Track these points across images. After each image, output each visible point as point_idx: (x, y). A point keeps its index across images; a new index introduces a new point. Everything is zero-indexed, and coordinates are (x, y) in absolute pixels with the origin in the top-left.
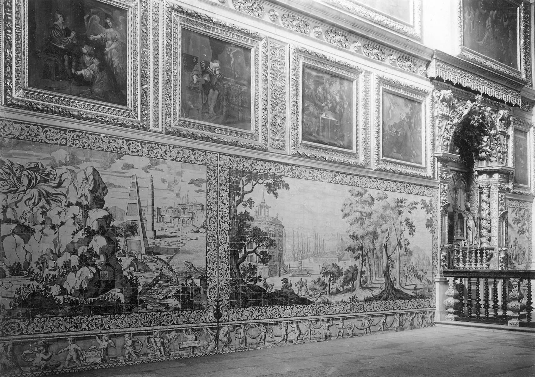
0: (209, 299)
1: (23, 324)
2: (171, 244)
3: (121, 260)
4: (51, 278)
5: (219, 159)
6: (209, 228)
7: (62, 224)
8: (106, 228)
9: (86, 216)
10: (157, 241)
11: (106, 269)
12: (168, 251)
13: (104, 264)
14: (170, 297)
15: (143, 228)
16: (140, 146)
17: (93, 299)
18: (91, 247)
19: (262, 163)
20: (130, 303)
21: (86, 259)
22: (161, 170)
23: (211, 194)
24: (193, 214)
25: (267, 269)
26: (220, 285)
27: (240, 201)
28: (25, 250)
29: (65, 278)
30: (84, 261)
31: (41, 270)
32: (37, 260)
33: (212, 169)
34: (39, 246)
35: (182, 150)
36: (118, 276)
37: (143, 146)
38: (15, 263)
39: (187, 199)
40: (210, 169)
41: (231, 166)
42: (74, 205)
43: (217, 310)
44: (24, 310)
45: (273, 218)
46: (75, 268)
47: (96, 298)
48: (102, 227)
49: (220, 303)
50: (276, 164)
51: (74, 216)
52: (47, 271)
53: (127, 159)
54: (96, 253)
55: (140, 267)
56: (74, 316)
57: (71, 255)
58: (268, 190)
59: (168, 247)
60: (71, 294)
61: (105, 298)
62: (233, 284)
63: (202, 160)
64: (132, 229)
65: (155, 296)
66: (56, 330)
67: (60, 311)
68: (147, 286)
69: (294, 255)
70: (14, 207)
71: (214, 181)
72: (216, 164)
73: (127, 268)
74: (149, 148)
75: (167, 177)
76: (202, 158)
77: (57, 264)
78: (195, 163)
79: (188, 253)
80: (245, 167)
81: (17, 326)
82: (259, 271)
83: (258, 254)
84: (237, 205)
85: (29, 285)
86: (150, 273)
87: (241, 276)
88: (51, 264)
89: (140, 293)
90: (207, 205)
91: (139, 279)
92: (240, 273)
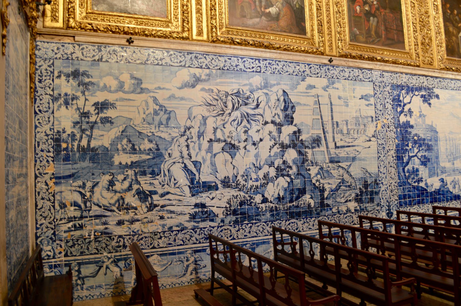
0: (382, 200)
1: (234, 230)
2: (349, 153)
3: (309, 170)
4: (255, 189)
5: (382, 76)
6: (379, 137)
7: (261, 140)
8: (296, 142)
9: (280, 132)
10: (338, 151)
12: (347, 159)
13: (296, 174)
14: (350, 200)
15: (326, 140)
16: (319, 69)
17: (289, 205)
19: (417, 77)
20: (319, 207)
21: (282, 170)
22: (338, 89)
23: (378, 106)
25: (427, 170)
26: (390, 187)
27: (402, 112)
30: (280, 172)
31: (246, 182)
32: (243, 173)
33: (378, 85)
34: (244, 160)
35: (353, 71)
36: (308, 183)
37: (322, 68)
38: (225, 177)
40: (376, 85)
41: (392, 82)
43: (388, 210)
44: (234, 218)
45: (429, 125)
46: (273, 178)
48: (293, 141)
49: (391, 203)
50: (428, 78)
51: (270, 132)
52: (251, 183)
53: (310, 81)
55: (326, 175)
56: (274, 221)
57: (270, 167)
58: (424, 101)
59: (347, 156)
60: (271, 202)
62: (401, 186)
63: (369, 78)
64: (317, 141)
65: (338, 200)
66: (260, 234)
67: (263, 217)
68: (332, 191)
69: (447, 157)
71: (380, 96)
72: (380, 80)
73: (314, 177)
74: (327, 71)
75: (342, 94)
76: (369, 76)
77: (258, 176)
78: (364, 81)
79: (364, 160)
80: (403, 82)
81: (229, 232)
82: (420, 173)
83: (420, 158)
84: (400, 115)
85: (237, 196)
87: (407, 178)
88: (254, 176)
89: (327, 198)
90: (376, 117)
92: (405, 175)
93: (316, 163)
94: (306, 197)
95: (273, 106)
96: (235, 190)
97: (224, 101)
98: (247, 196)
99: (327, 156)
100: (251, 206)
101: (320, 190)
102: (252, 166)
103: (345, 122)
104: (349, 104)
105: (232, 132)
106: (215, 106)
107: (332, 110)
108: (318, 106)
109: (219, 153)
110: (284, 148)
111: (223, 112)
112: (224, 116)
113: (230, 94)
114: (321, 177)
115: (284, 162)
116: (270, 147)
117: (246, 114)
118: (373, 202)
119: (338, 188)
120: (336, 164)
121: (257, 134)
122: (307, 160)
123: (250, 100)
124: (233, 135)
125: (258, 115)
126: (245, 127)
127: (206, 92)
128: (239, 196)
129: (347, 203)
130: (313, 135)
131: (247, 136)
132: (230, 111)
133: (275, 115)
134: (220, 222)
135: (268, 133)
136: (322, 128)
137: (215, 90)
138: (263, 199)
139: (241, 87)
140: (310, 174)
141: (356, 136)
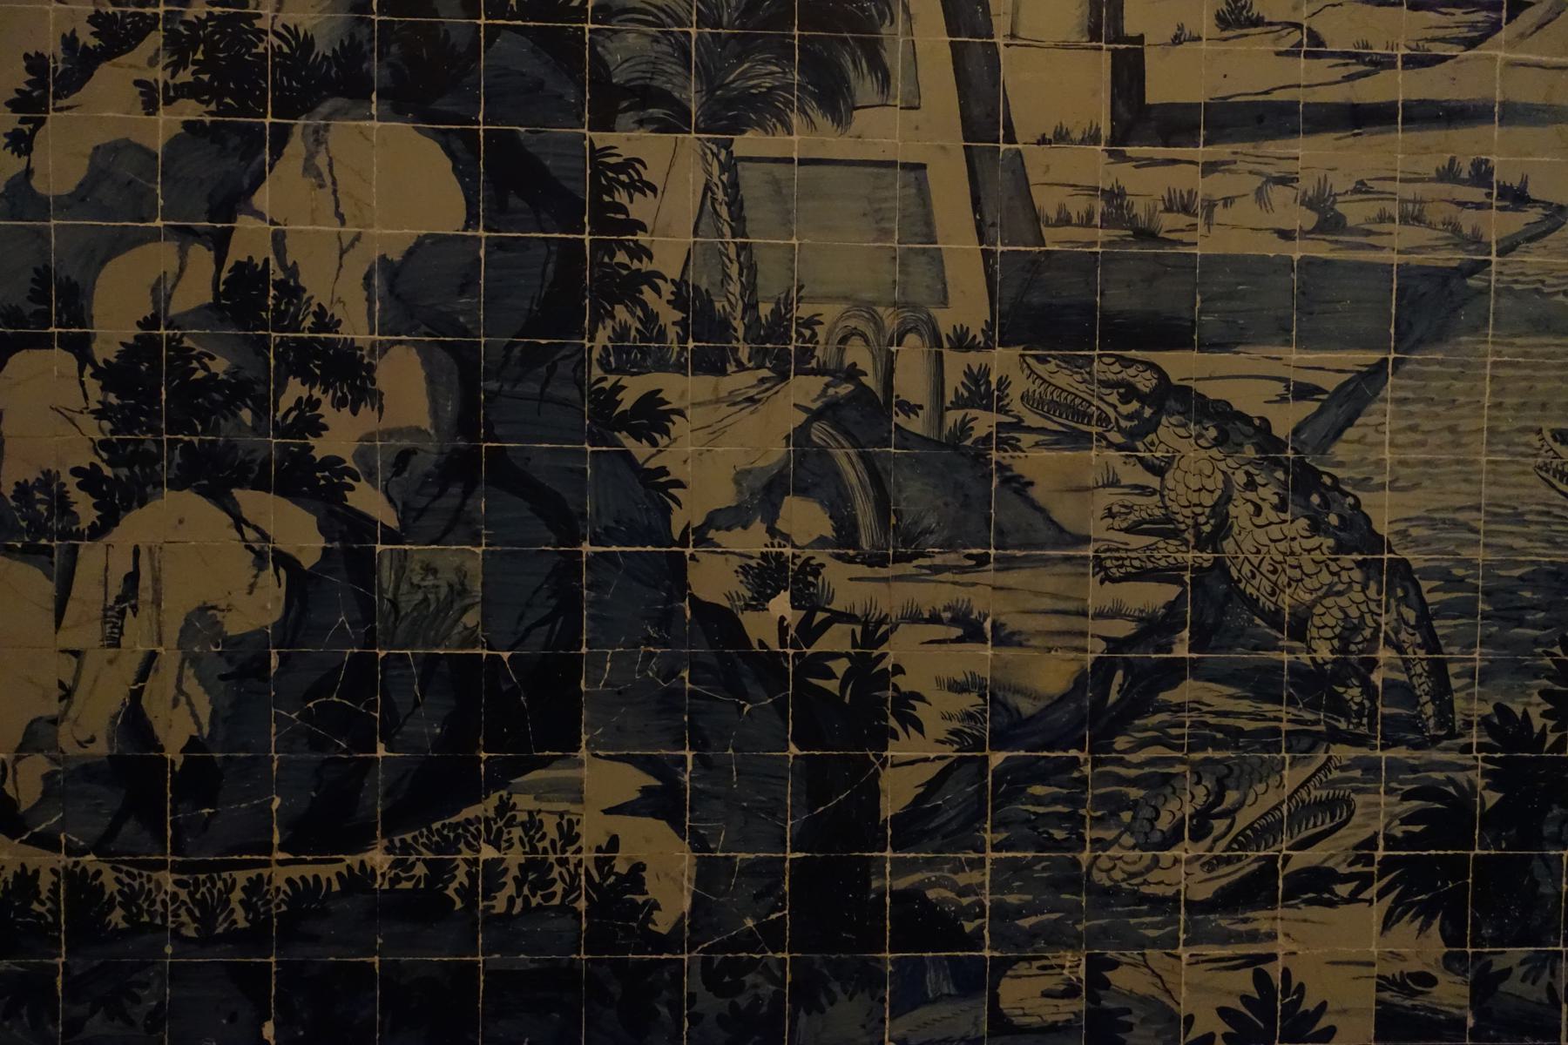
2: (1355, 212)
3: (653, 417)
10: (1150, 180)
11: (458, 527)
12: (1306, 301)
13: (425, 462)
17: (282, 874)
18: (262, 251)
20: (771, 935)
21: (200, 401)
46: (62, 505)
47: (327, 872)
54: (324, 321)
59: (1321, 250)
61: (440, 871)
65: (1114, 858)
73: (734, 518)
86: (1048, 580)
89: (913, 826)
93: (778, 327)
94: (575, 793)
110: (250, 101)
114: (845, 536)
116: (20, 77)
119: (1124, 687)
120: (1104, 367)
122: (628, 287)
129: (1262, 920)
140: (658, 487)
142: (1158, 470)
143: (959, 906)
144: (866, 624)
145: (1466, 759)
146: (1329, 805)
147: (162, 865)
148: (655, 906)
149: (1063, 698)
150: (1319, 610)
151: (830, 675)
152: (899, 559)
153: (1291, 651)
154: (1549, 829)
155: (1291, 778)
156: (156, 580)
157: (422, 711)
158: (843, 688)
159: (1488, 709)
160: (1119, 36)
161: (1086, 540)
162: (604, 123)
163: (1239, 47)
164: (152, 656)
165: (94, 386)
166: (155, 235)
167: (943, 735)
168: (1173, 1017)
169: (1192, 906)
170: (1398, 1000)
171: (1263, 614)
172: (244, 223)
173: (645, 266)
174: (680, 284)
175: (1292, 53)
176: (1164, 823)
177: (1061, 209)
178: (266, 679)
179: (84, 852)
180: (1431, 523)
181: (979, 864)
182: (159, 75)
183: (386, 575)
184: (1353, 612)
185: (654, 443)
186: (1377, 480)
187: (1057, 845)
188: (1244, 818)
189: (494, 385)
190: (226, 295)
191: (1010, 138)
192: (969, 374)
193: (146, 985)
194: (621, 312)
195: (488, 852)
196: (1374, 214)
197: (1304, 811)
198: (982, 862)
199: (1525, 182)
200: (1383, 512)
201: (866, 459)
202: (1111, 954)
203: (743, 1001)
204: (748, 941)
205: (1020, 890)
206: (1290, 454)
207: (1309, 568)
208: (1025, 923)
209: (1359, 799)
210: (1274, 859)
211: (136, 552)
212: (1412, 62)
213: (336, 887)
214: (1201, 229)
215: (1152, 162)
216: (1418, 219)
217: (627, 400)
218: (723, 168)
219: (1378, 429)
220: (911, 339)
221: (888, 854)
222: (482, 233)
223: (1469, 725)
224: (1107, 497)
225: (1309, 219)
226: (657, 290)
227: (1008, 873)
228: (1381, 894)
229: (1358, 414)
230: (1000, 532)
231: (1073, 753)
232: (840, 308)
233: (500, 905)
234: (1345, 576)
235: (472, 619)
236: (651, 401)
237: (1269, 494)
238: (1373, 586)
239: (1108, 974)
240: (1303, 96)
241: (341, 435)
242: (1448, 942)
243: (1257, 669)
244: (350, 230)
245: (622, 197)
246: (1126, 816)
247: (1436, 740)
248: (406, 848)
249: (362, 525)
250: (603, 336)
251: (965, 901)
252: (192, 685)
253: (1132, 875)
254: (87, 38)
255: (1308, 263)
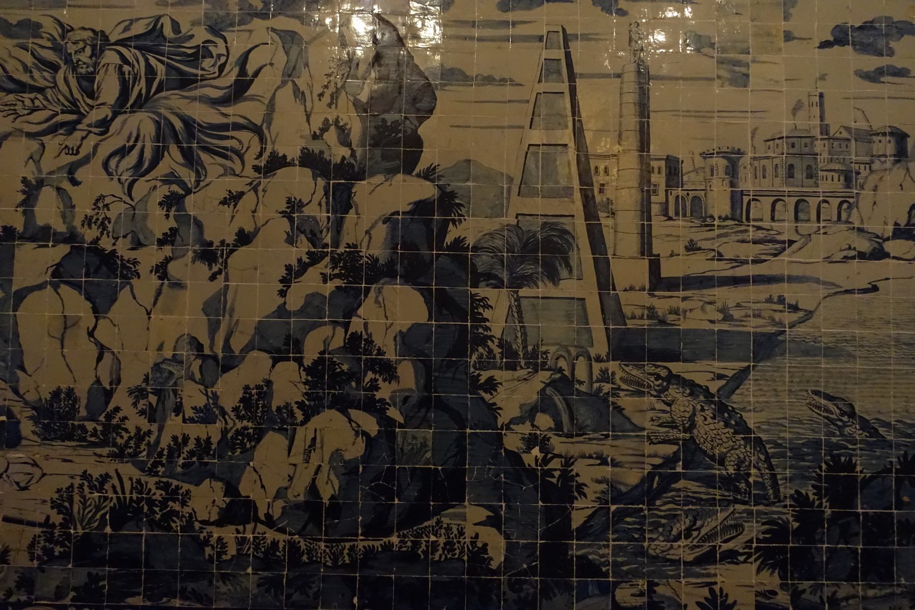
2: (736, 314)
3: (491, 386)
4: (192, 453)
7: (244, 238)
8: (425, 249)
9: (342, 202)
10: (663, 303)
11: (424, 423)
12: (721, 345)
13: (413, 400)
17: (362, 544)
20: (532, 571)
21: (339, 379)
24: (848, 178)
28: (97, 343)
29: (248, 453)
30: (330, 386)
31: (152, 420)
32: (138, 381)
34: (150, 326)
38: (56, 394)
39: (816, 111)
42: (291, 164)
44: (80, 576)
46: (292, 414)
47: (377, 544)
51: (294, 206)
52: (174, 425)
54: (380, 352)
55: (584, 415)
57: (275, 361)
59: (725, 327)
60: (269, 522)
61: (416, 544)
64: (543, 251)
65: (657, 545)
67: (223, 589)
70: (66, 185)
73: (519, 420)
77: (215, 397)
85: (105, 478)
88: (193, 396)
89: (584, 532)
91: (578, 467)
93: (535, 354)
94: (464, 517)
95: (318, 90)
96: (99, 451)
97: (83, 71)
98: (151, 482)
99: (597, 326)
100: (169, 529)
101: (547, 486)
102: (185, 352)
103: (722, 163)
104: (753, 70)
105: (108, 200)
106: (41, 90)
107: (643, 109)
108: (565, 87)
109: (40, 287)
110: (358, 280)
111: (73, 117)
112: (78, 135)
113: (113, 39)
114: (558, 427)
115: (354, 343)
116: (283, 272)
117: (178, 125)
118: (887, 577)
119: (657, 484)
120: (649, 368)
121: (227, 211)
122: (483, 341)
123: (207, 63)
124: (112, 214)
125: (237, 127)
126: (171, 179)
127: (10, 36)
128: (116, 481)
129: (711, 569)
130: (525, 223)
131: (176, 218)
132: (106, 112)
133: (325, 129)
134: (12, 585)
135: (283, 207)
136: (576, 184)
137: (50, 27)
138: (230, 505)
139: (169, 10)
140: (493, 410)
141: (786, 228)
142: (669, 405)
143: (601, 562)
144: (566, 458)
145: (785, 510)
146: (735, 527)
147: (320, 540)
148: (491, 559)
149: (637, 486)
150: (729, 455)
151: (553, 477)
152: (577, 435)
153: (719, 470)
154: (817, 537)
155: (721, 516)
156: (322, 440)
157: (411, 487)
158: (558, 481)
159: (793, 492)
160: (651, 254)
161: (643, 429)
162: (475, 285)
163: (693, 257)
164: (320, 466)
165: (303, 374)
166: (325, 324)
167: (594, 499)
168: (679, 605)
169: (686, 563)
170: (763, 600)
171: (708, 456)
172: (354, 319)
173: (489, 333)
174: (501, 340)
175: (712, 259)
176: (675, 532)
177: (633, 313)
178: (358, 475)
179: (294, 534)
180: (769, 423)
181: (607, 546)
182: (328, 271)
183: (399, 440)
184: (741, 456)
185: (492, 394)
186: (748, 408)
187: (636, 540)
188: (704, 531)
189: (437, 374)
190: (348, 343)
191: (614, 289)
192: (601, 370)
193: (313, 583)
194: (481, 349)
195: (433, 538)
196: (743, 314)
197: (726, 529)
198: (608, 546)
199: (797, 303)
200: (751, 420)
201: (566, 400)
202: (656, 580)
203: (522, 595)
204: (525, 573)
205: (622, 556)
206: (716, 399)
207: (725, 440)
208: (625, 568)
209: (746, 525)
210: (715, 546)
211: (316, 430)
212: (754, 262)
213: (380, 549)
214: (682, 320)
215: (665, 297)
216: (759, 316)
217: (482, 379)
218: (515, 300)
219: (747, 390)
220: (581, 358)
221: (574, 542)
222: (433, 322)
223: (786, 497)
224: (650, 414)
225: (720, 316)
226: (493, 342)
227: (618, 550)
228: (756, 560)
229: (740, 385)
230: (613, 426)
231: (641, 506)
232: (555, 348)
233: (437, 558)
234: (738, 443)
235: (429, 455)
236: (491, 379)
237: (709, 413)
238: (748, 447)
239: (656, 588)
240: (716, 274)
241: (385, 391)
242: (781, 579)
243: (707, 476)
244: (389, 322)
245: (481, 310)
246: (661, 530)
247: (774, 503)
248: (404, 536)
249: (391, 422)
250: (474, 357)
251: (603, 560)
252: (333, 477)
253: (663, 551)
254: (305, 259)
255: (720, 331)
